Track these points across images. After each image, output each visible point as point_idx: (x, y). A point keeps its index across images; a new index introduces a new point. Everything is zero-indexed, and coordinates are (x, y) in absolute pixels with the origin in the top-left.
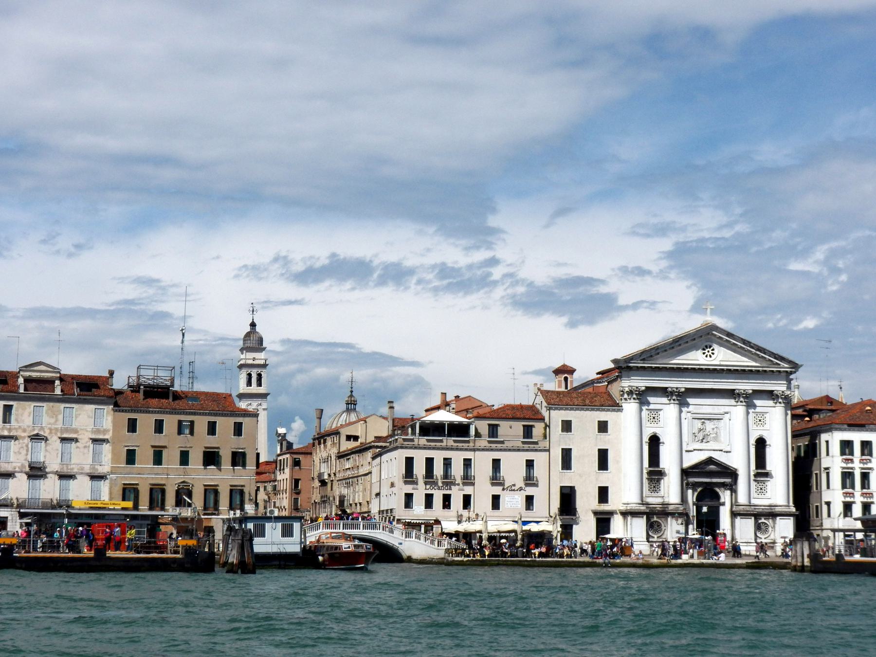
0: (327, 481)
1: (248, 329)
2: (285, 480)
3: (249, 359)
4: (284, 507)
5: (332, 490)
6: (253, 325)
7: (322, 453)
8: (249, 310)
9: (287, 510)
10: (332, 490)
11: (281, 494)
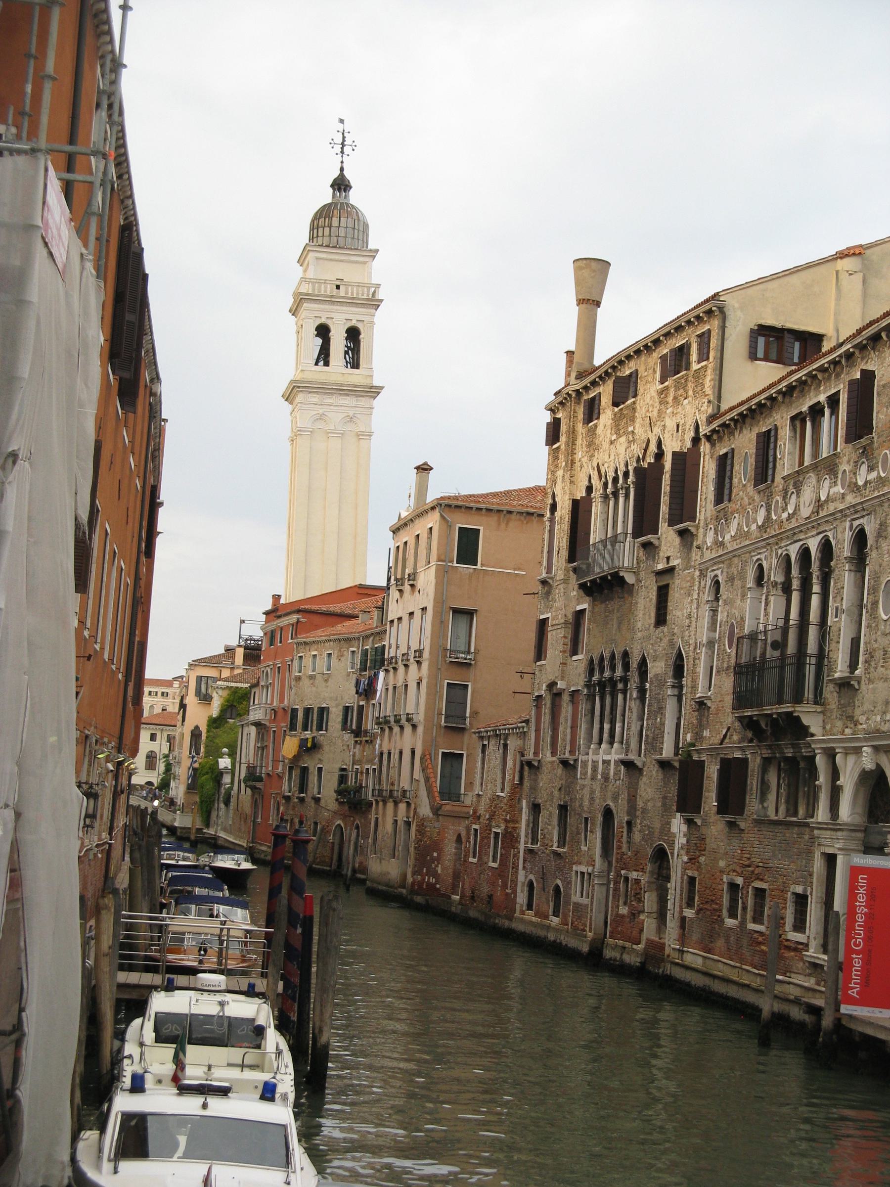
0: (630, 579)
1: (326, 196)
2: (418, 614)
4: (409, 720)
5: (661, 619)
6: (341, 185)
7: (601, 457)
8: (332, 143)
9: (420, 730)
10: (661, 619)
11: (401, 669)
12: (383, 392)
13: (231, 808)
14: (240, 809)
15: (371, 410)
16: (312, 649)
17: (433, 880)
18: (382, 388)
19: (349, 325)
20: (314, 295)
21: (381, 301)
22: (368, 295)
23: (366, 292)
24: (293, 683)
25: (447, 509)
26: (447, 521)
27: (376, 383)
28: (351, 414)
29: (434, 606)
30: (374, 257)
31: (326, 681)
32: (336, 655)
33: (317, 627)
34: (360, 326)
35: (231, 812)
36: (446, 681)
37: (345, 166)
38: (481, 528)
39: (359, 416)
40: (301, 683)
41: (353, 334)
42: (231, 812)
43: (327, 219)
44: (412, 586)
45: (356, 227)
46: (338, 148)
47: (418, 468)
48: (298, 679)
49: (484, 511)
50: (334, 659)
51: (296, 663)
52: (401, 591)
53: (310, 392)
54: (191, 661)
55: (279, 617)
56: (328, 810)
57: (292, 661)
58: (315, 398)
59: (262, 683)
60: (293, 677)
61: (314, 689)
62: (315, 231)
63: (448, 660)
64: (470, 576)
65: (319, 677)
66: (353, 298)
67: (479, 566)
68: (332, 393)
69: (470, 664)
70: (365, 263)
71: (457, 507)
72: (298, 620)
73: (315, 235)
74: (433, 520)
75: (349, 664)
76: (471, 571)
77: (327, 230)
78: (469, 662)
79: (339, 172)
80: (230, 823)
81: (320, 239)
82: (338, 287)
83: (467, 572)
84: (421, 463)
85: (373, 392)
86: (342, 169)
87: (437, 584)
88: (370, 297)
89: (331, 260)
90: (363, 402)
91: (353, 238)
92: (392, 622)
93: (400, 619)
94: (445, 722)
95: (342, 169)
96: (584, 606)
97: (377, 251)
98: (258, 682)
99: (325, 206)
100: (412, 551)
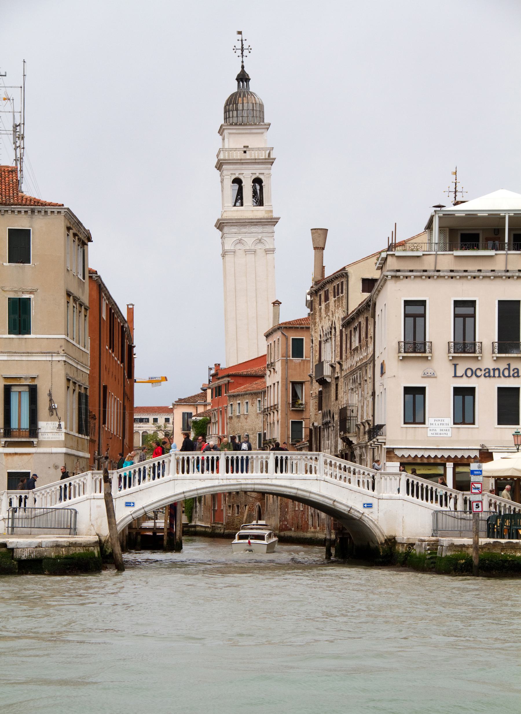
1: (233, 87)
2: (276, 384)
3: (236, 149)
8: (235, 49)
11: (272, 413)
12: (280, 221)
13: (202, 504)
14: (206, 504)
15: (273, 234)
16: (238, 399)
17: (286, 523)
18: (279, 218)
19: (254, 177)
20: (229, 160)
21: (274, 159)
22: (265, 156)
23: (264, 154)
24: (228, 421)
25: (285, 329)
26: (285, 336)
27: (275, 215)
28: (260, 237)
29: (282, 381)
30: (268, 129)
31: (246, 419)
32: (250, 403)
33: (241, 385)
34: (261, 177)
35: (202, 507)
36: (291, 420)
37: (244, 64)
38: (304, 338)
39: (265, 239)
40: (233, 421)
41: (258, 181)
42: (202, 507)
43: (234, 105)
44: (274, 369)
45: (255, 108)
46: (240, 52)
47: (274, 303)
48: (231, 418)
49: (305, 328)
50: (249, 404)
51: (229, 408)
52: (270, 371)
53: (231, 226)
54: (174, 403)
55: (219, 379)
56: (252, 497)
57: (227, 407)
58: (234, 230)
59: (213, 421)
60: (228, 417)
61: (240, 424)
62: (228, 113)
63: (291, 409)
64: (300, 364)
65: (242, 416)
66: (256, 159)
67: (304, 358)
68: (246, 225)
69: (303, 410)
70: (262, 133)
71: (290, 328)
72: (228, 381)
73: (228, 117)
74: (278, 335)
75: (258, 409)
76: (300, 361)
77: (235, 112)
78: (302, 409)
79: (241, 69)
80: (203, 514)
81: (231, 119)
82: (245, 152)
83: (298, 361)
84: (275, 301)
85: (273, 222)
86: (243, 67)
87: (282, 370)
88: (267, 157)
89: (239, 134)
90: (268, 229)
91: (253, 117)
92: (268, 387)
93: (270, 386)
94: (292, 442)
95: (243, 67)
96: (321, 389)
97: (269, 125)
98: (210, 420)
99: (232, 95)
100: (273, 349)
